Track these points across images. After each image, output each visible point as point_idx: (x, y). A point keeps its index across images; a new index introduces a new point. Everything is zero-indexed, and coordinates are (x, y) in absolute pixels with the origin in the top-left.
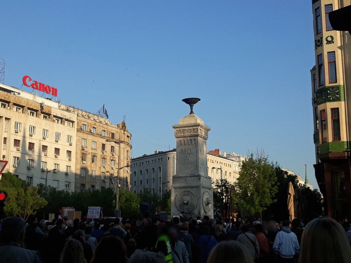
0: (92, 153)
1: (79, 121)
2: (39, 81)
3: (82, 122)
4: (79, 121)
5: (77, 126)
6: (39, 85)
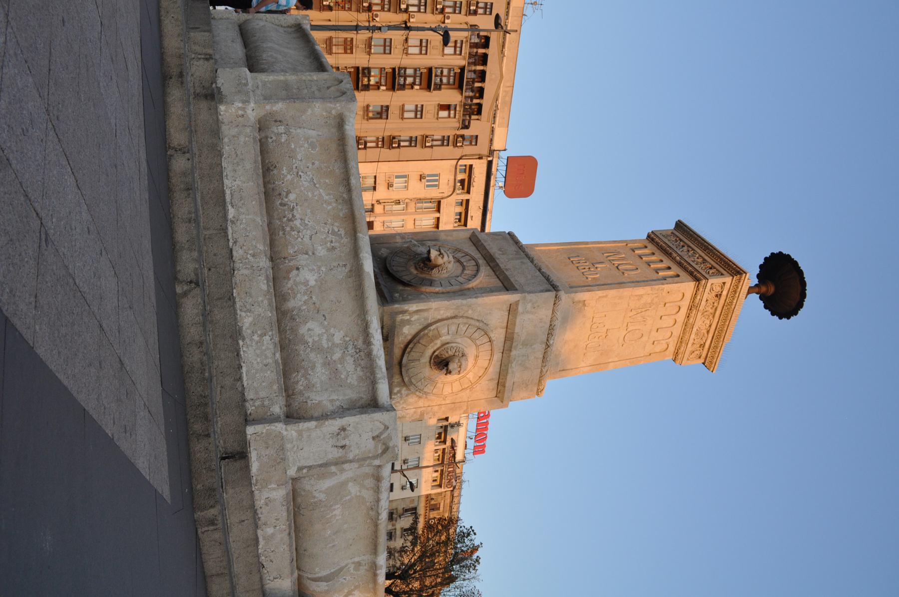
0: (395, 529)
1: (443, 496)
2: (490, 420)
3: (443, 501)
4: (443, 495)
5: (435, 494)
6: (485, 421)
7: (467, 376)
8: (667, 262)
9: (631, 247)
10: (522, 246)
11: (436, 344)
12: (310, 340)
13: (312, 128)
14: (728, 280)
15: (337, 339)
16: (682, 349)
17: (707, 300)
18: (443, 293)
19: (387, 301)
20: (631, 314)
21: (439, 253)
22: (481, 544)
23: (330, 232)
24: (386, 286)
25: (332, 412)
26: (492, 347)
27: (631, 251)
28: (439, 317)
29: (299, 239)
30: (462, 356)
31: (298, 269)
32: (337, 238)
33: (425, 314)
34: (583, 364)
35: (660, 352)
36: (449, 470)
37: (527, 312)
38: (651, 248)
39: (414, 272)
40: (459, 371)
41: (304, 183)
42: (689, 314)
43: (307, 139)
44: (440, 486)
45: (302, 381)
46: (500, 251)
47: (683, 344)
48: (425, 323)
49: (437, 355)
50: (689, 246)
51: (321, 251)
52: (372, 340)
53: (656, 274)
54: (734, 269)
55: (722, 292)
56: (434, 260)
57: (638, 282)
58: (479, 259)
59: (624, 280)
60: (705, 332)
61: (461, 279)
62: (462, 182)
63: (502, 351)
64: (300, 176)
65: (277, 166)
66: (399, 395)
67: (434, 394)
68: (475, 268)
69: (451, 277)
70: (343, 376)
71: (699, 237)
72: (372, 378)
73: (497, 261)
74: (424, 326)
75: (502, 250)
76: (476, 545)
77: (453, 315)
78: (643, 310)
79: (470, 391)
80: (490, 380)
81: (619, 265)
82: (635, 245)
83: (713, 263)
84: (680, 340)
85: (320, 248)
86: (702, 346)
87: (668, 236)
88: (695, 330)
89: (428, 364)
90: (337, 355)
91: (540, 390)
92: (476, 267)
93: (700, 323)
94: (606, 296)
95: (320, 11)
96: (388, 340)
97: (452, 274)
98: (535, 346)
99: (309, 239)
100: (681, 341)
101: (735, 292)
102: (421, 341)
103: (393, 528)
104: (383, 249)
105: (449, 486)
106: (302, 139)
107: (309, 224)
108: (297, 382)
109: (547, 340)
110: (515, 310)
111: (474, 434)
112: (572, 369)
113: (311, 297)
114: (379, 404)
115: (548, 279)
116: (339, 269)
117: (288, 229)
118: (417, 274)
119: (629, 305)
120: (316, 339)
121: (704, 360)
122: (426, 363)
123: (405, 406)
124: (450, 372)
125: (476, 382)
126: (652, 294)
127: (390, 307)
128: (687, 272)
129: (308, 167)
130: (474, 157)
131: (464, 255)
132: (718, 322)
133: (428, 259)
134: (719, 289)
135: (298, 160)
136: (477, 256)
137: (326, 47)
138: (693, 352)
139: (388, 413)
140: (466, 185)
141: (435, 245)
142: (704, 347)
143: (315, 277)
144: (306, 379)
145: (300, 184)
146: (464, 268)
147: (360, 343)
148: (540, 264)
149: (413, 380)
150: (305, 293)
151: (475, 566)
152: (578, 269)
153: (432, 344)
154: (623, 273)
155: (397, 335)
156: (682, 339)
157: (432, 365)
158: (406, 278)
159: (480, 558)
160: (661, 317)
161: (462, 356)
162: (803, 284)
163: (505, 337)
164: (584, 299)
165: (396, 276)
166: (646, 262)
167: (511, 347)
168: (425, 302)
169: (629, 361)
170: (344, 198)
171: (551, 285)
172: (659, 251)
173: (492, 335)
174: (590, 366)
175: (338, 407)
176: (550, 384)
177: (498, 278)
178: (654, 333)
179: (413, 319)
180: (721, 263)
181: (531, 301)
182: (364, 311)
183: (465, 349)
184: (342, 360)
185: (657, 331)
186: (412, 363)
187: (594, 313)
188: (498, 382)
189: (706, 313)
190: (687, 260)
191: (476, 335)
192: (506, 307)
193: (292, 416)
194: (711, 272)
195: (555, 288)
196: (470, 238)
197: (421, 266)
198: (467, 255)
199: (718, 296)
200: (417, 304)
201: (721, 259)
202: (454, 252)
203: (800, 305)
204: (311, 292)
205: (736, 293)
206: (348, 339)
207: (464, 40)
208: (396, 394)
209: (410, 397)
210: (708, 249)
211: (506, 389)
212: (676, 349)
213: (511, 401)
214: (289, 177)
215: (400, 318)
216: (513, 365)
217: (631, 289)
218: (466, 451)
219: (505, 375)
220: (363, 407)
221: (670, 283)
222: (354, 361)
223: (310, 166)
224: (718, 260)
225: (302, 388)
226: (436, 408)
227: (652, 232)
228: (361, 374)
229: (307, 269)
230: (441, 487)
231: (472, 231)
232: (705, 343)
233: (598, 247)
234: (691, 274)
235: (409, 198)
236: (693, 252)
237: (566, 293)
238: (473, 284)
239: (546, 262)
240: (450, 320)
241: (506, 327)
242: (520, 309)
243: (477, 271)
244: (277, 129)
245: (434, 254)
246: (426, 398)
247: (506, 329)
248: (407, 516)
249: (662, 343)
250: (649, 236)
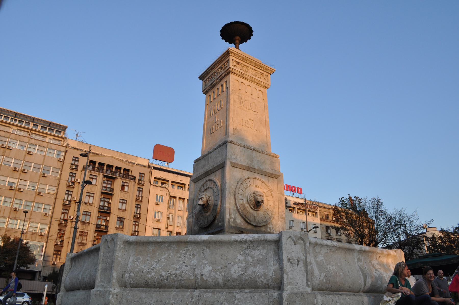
0: (336, 238)
1: (321, 212)
3: (324, 212)
4: (321, 212)
5: (320, 216)
7: (265, 192)
8: (219, 86)
9: (209, 103)
10: (202, 157)
11: (247, 206)
12: (241, 272)
13: (128, 258)
14: (231, 58)
15: (242, 258)
16: (262, 84)
17: (240, 69)
18: (222, 200)
19: (222, 229)
20: (242, 106)
21: (201, 199)
22: (348, 195)
23: (185, 255)
24: (215, 229)
25: (279, 265)
27: (211, 103)
28: (234, 203)
29: (187, 272)
30: (255, 193)
31: (202, 275)
32: (188, 252)
33: (232, 210)
34: (265, 133)
35: (263, 95)
36: (308, 207)
37: (236, 158)
38: (211, 93)
39: (209, 213)
40: (263, 196)
41: (157, 266)
42: (246, 78)
43: (134, 262)
44: (316, 213)
45: (262, 279)
46: (203, 168)
47: (260, 83)
48: (236, 210)
49: (253, 207)
50: (212, 75)
51: (194, 261)
52: (244, 239)
53: (224, 92)
54: (226, 54)
55: (237, 61)
56: (204, 202)
57: (227, 101)
58: (206, 179)
59: (225, 108)
60: (255, 72)
61: (215, 190)
62: (162, 183)
63: (254, 173)
64: (153, 268)
65: (146, 280)
66: (271, 229)
67: (273, 211)
68: (210, 182)
69: (214, 194)
70: (261, 257)
71: (208, 69)
72: (263, 242)
73: (208, 170)
74: (237, 212)
75: (203, 167)
76: (349, 198)
77: (234, 196)
78: (241, 100)
79: (273, 192)
80: (268, 181)
81: (217, 110)
82: (208, 100)
83: (222, 64)
84: (258, 84)
85: (192, 262)
86: (262, 74)
87: (205, 84)
88: (254, 77)
89: (257, 212)
90: (250, 259)
91: (276, 156)
92: (210, 181)
93: (251, 73)
94: (233, 118)
95: (63, 247)
96: (243, 231)
97: (212, 194)
98: (254, 156)
99: (187, 267)
100: (258, 84)
101: (237, 55)
102: (245, 214)
103: (335, 240)
104: (195, 228)
105: (317, 208)
106: (134, 264)
107: (179, 266)
108: (262, 282)
109: (251, 150)
110: (234, 164)
111: (291, 192)
112: (267, 139)
113: (218, 269)
114: (278, 239)
115: (220, 146)
116: (205, 253)
117: (180, 278)
118: (210, 212)
119: (238, 107)
120: (240, 269)
121: (269, 74)
122: (256, 213)
123: (278, 226)
124: (263, 201)
125: (269, 188)
126: (234, 95)
127: (226, 228)
128: (225, 77)
129: (149, 263)
130: (151, 176)
131: (203, 186)
132: (251, 65)
133: (203, 205)
134: (235, 63)
135: (145, 268)
136: (204, 180)
137: (82, 246)
138: (264, 79)
139: (283, 235)
140: (164, 182)
141: (196, 201)
142: (262, 73)
143: (208, 266)
144: (261, 277)
145: (157, 268)
146: (210, 188)
147: (245, 246)
148: (212, 149)
149: (265, 221)
150: (216, 272)
151: (359, 199)
152: (217, 130)
153: (247, 208)
154: (222, 108)
156: (257, 84)
157: (258, 210)
158: (212, 218)
159: (356, 196)
160: (246, 92)
161: (255, 193)
162: (237, 22)
163: (248, 170)
164: (233, 129)
165: (210, 223)
166: (218, 96)
167: (253, 168)
168: (225, 210)
169: (266, 111)
170: (168, 246)
171: (224, 144)
172: (213, 89)
173: (246, 177)
174: (266, 130)
175: (277, 262)
176: (273, 151)
177: (217, 171)
178: (253, 97)
179: (233, 217)
180: (222, 60)
181: (231, 155)
182: (229, 242)
183: (251, 192)
184: (252, 257)
185: (253, 95)
186: (255, 220)
187: (240, 125)
188: (270, 177)
189: (246, 70)
190: (219, 76)
191: (245, 185)
192: (232, 169)
193: (280, 287)
194: (226, 65)
195: (225, 143)
196: (195, 183)
197: (206, 210)
198: (203, 185)
199: (238, 63)
200: (226, 214)
201: (220, 60)
202: (201, 192)
203: (247, 25)
204: (215, 269)
205: (238, 55)
206: (242, 253)
207: (90, 173)
208: (271, 230)
209: (273, 223)
210: (214, 65)
211: (273, 173)
212: (262, 87)
213: (280, 172)
214: (153, 274)
215: (232, 224)
216: (262, 168)
217: (230, 105)
218: (300, 197)
220: (278, 248)
221: (230, 86)
222: (254, 250)
223: (148, 262)
224: (221, 61)
225: (265, 280)
226: (280, 210)
227: (203, 91)
228: (261, 247)
229: (203, 270)
230: (317, 212)
231: (191, 181)
232: (261, 73)
233: (207, 119)
234: (226, 75)
235: (167, 212)
236: (215, 73)
237: (228, 137)
238: (219, 184)
239: (212, 146)
240: (236, 198)
241: (242, 170)
242: (234, 161)
243: (212, 181)
244: (127, 277)
245: (201, 202)
246: (274, 215)
247: (244, 170)
248: (330, 231)
249: (259, 93)
250: (205, 93)
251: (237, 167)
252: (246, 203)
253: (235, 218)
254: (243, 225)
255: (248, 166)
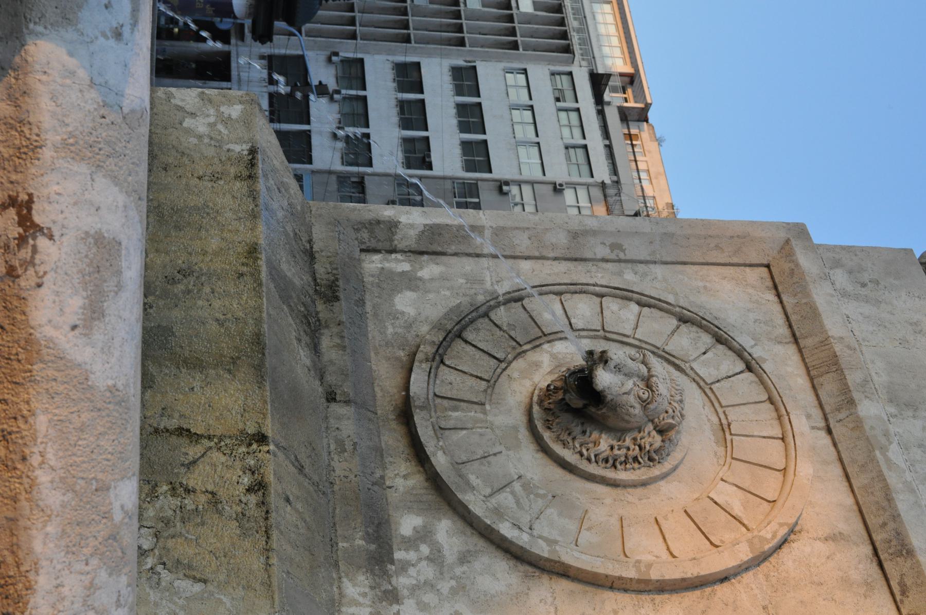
11: (537, 365)
26: (766, 388)
63: (822, 424)
66: (425, 549)
96: (337, 299)
122: (515, 428)
155: (376, 315)
167: (845, 390)
186: (455, 409)
208: (411, 543)
219: (885, 504)
251: (785, 298)
252: (553, 356)
253: (419, 283)
254: (390, 330)
255: (837, 349)
